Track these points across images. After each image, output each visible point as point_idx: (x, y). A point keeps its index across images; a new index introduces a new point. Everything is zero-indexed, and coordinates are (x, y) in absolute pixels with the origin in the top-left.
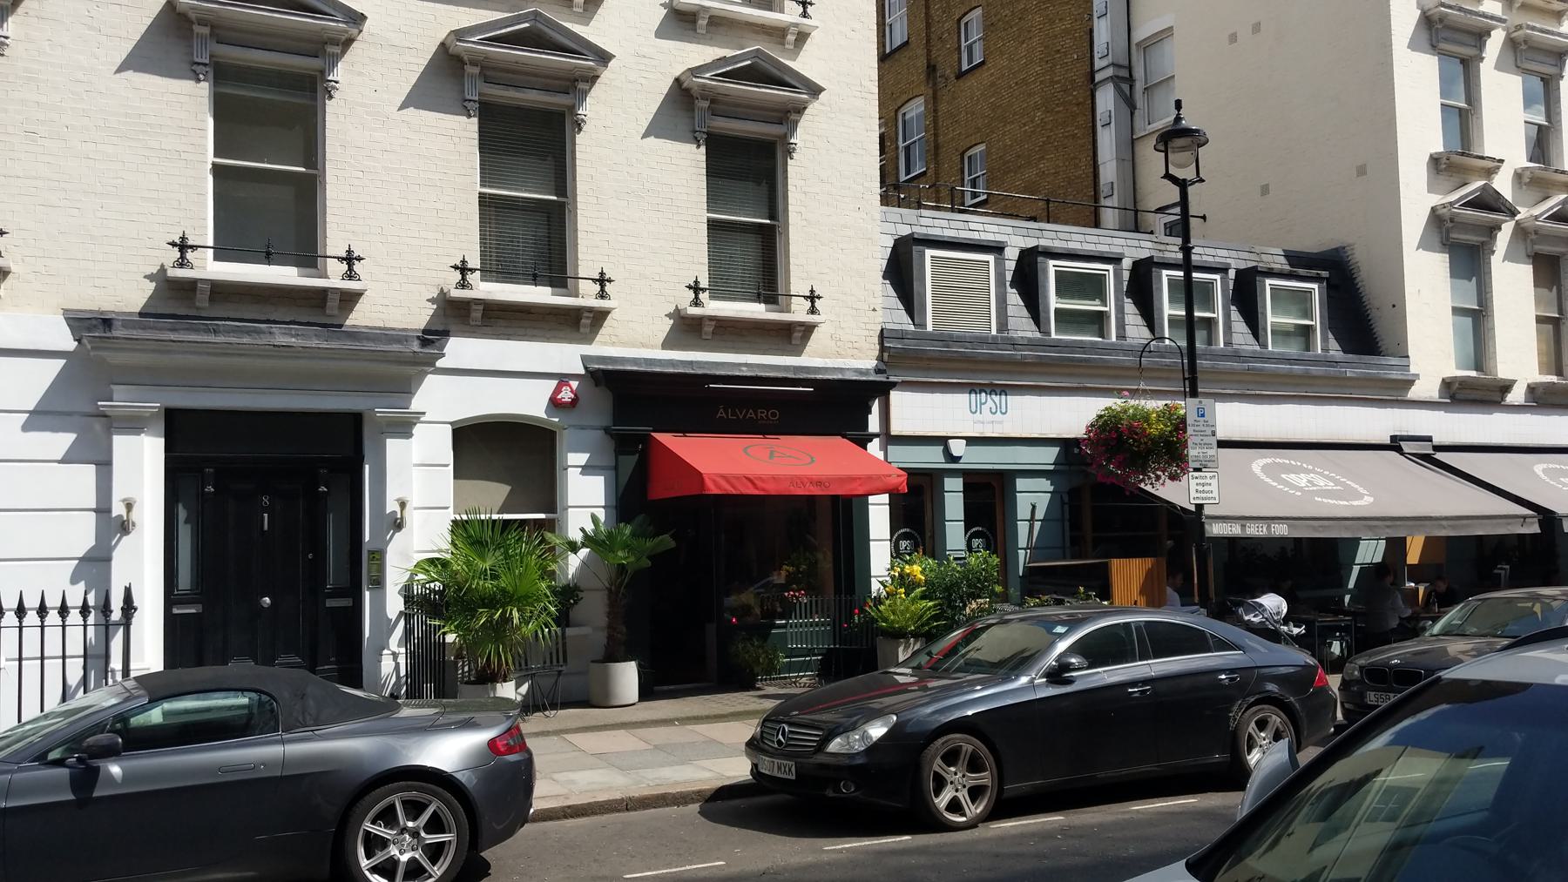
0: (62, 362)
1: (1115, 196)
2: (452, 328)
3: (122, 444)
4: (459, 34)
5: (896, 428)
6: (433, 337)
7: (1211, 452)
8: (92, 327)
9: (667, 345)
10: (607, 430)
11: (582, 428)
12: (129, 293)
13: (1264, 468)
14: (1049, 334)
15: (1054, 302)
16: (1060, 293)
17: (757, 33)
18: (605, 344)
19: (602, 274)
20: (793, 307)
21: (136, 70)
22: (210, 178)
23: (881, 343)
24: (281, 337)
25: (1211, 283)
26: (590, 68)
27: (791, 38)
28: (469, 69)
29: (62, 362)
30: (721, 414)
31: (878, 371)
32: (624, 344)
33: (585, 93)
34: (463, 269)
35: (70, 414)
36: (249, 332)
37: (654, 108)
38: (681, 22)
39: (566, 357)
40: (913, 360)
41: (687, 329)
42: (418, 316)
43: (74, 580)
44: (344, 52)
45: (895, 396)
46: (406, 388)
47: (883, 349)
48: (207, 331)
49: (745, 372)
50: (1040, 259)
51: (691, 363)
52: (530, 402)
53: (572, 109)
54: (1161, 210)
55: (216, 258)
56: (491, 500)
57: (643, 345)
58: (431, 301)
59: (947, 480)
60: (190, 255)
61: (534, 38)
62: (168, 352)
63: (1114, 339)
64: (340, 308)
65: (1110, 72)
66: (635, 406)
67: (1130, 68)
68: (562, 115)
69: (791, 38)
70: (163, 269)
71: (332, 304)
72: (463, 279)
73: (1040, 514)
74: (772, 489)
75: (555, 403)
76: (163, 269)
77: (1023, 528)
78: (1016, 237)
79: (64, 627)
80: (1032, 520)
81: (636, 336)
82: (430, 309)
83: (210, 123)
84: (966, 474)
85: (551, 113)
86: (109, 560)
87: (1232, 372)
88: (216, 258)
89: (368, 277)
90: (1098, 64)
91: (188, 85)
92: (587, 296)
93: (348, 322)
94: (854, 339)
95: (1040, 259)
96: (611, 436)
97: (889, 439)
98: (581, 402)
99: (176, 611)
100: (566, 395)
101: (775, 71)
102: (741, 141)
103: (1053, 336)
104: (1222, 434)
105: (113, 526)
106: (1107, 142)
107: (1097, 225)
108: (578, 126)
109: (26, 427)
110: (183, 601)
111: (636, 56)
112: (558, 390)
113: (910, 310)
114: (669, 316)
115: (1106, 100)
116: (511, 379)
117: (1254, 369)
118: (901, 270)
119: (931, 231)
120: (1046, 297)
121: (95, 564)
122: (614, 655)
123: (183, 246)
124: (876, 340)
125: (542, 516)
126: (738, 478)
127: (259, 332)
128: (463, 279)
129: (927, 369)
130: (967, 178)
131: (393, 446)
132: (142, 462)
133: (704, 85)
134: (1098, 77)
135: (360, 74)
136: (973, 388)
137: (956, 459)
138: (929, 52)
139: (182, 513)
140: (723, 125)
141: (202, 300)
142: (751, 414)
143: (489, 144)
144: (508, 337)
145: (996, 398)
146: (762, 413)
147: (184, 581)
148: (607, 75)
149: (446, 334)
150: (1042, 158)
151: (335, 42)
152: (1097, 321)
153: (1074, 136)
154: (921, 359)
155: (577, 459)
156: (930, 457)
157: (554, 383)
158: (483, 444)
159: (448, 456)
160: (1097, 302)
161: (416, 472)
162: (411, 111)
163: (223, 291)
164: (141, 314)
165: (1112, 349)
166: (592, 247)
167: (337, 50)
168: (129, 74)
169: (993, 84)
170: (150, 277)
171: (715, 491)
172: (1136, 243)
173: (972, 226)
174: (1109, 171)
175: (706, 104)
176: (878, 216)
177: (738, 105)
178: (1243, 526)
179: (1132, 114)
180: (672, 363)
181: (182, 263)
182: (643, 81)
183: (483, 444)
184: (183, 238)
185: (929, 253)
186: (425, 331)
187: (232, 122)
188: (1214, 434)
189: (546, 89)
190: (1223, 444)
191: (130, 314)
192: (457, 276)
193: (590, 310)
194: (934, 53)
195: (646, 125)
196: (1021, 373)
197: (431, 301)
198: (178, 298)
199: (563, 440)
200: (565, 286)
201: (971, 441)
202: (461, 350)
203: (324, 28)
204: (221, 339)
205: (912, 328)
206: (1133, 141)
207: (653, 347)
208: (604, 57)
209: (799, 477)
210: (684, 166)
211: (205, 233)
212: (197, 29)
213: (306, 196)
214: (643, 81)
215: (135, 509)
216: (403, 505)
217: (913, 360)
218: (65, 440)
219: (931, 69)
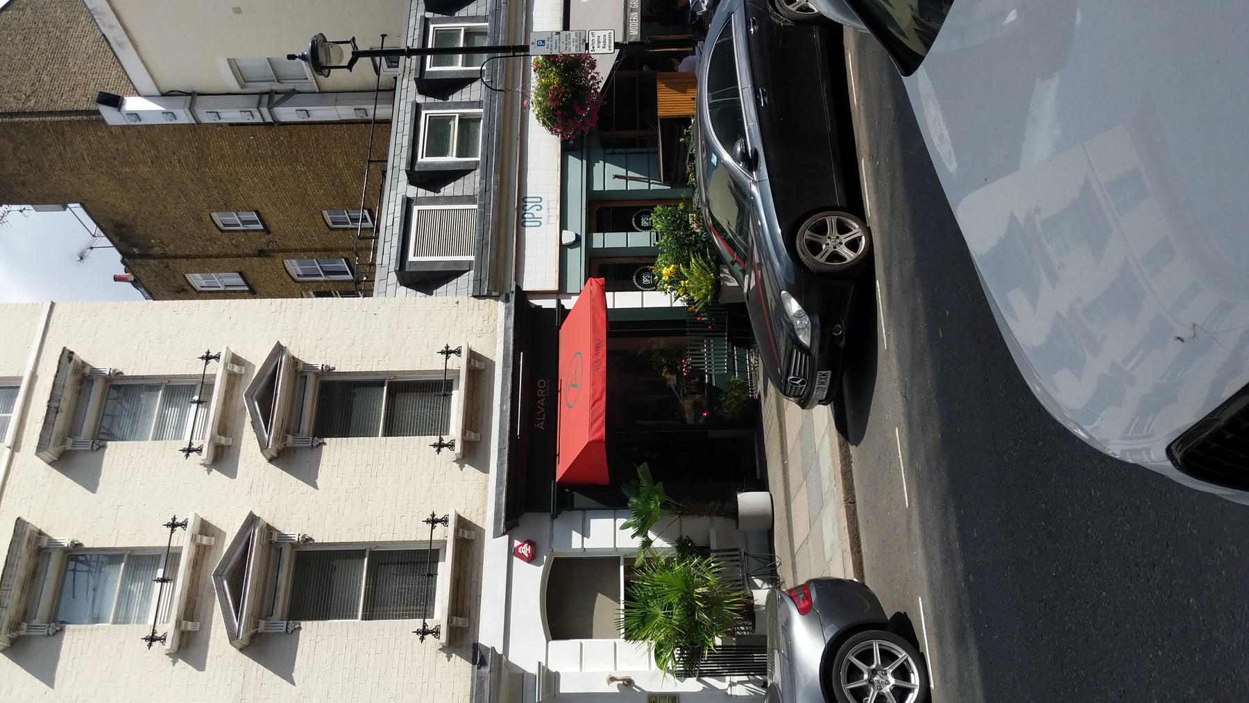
2: (471, 641)
4: (233, 637)
5: (554, 286)
6: (478, 656)
7: (573, 35)
9: (484, 468)
10: (554, 517)
11: (552, 536)
14: (477, 162)
15: (451, 158)
16: (444, 153)
17: (232, 397)
18: (484, 519)
19: (428, 521)
23: (484, 297)
25: (436, 31)
26: (261, 530)
27: (236, 369)
28: (261, 628)
30: (541, 426)
31: (507, 300)
32: (484, 504)
33: (281, 535)
34: (423, 632)
39: (494, 550)
40: (498, 273)
41: (472, 453)
42: (461, 668)
45: (526, 287)
46: (519, 677)
47: (489, 296)
49: (508, 406)
50: (417, 169)
51: (500, 450)
52: (530, 578)
53: (294, 545)
54: (377, 71)
58: (449, 658)
63: (481, 110)
65: (265, 110)
66: (535, 495)
67: (261, 94)
69: (236, 369)
72: (431, 632)
73: (622, 172)
74: (601, 385)
75: (532, 559)
77: (633, 186)
78: (399, 188)
80: (626, 178)
81: (478, 494)
82: (456, 658)
84: (590, 230)
90: (258, 119)
92: (446, 534)
95: (417, 169)
97: (562, 291)
100: (526, 550)
102: (319, 410)
103: (479, 159)
104: (558, 26)
106: (321, 113)
107: (389, 122)
108: (307, 540)
112: (521, 556)
113: (458, 274)
114: (462, 467)
115: (287, 113)
116: (512, 593)
118: (427, 281)
119: (394, 256)
120: (447, 164)
124: (482, 301)
125: (622, 568)
126: (592, 414)
128: (431, 632)
129: (506, 260)
130: (351, 226)
131: (565, 687)
133: (275, 439)
134: (269, 119)
136: (521, 224)
137: (578, 238)
138: (247, 255)
142: (541, 402)
144: (478, 596)
145: (529, 205)
148: (266, 517)
149: (476, 646)
150: (335, 165)
152: (467, 123)
154: (497, 266)
156: (576, 259)
157: (516, 559)
158: (565, 615)
159: (574, 643)
160: (451, 123)
161: (586, 669)
162: (295, 675)
165: (490, 112)
169: (274, 204)
172: (404, 92)
173: (389, 223)
174: (345, 112)
175: (290, 438)
176: (381, 299)
178: (632, 10)
180: (499, 466)
182: (271, 488)
183: (565, 615)
185: (411, 258)
186: (474, 663)
188: (558, 33)
190: (566, 26)
192: (429, 637)
193: (456, 531)
195: (306, 486)
196: (509, 184)
197: (449, 658)
200: (437, 551)
201: (563, 225)
202: (489, 634)
205: (472, 272)
207: (487, 481)
208: (252, 520)
214: (271, 488)
216: (612, 679)
217: (498, 273)
219: (261, 253)
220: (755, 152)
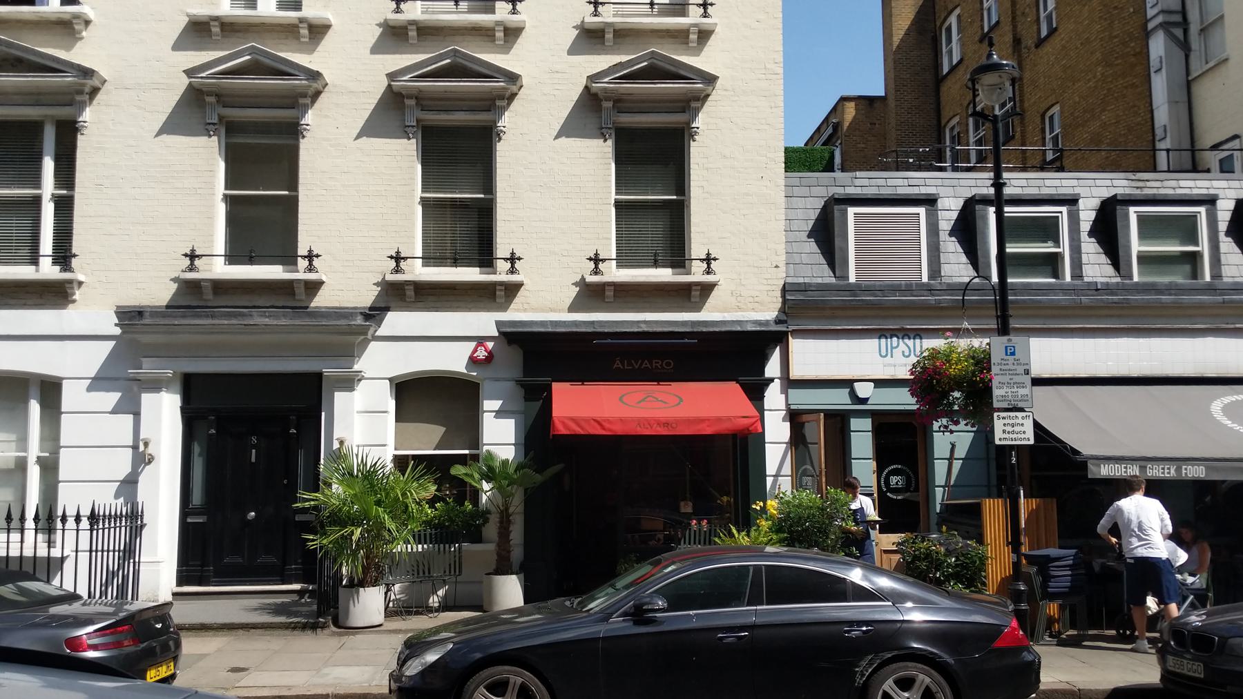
0: (114, 343)
1: (1168, 139)
2: (392, 305)
3: (147, 399)
4: (593, 78)
5: (796, 373)
6: (375, 313)
7: (1022, 391)
8: (130, 317)
9: (573, 308)
10: (519, 383)
11: (497, 380)
12: (160, 293)
13: (1226, 410)
14: (1131, 277)
15: (1136, 246)
16: (1143, 236)
17: (662, 37)
18: (518, 310)
19: (513, 254)
20: (693, 269)
21: (168, 134)
22: (613, 210)
23: (783, 296)
24: (258, 319)
25: (1193, 218)
26: (504, 88)
27: (693, 37)
28: (408, 102)
29: (114, 343)
30: (618, 364)
31: (778, 321)
32: (534, 310)
33: (697, 110)
34: (596, 260)
35: (116, 379)
36: (235, 316)
37: (366, 115)
38: (591, 38)
39: (484, 323)
40: (807, 310)
41: (592, 294)
42: (366, 296)
43: (117, 496)
44: (509, 105)
45: (795, 344)
46: (351, 352)
47: (785, 301)
48: (207, 316)
49: (645, 328)
50: (978, 207)
51: (593, 323)
52: (453, 360)
53: (688, 124)
54: (1215, 147)
55: (619, 266)
56: (427, 441)
57: (552, 310)
58: (377, 284)
59: (853, 421)
60: (601, 266)
61: (459, 70)
62: (172, 333)
63: (1068, 278)
64: (307, 294)
65: (1160, 19)
66: (542, 358)
67: (1184, 12)
68: (682, 130)
69: (693, 37)
70: (583, 279)
71: (300, 291)
72: (596, 267)
73: (961, 452)
74: (619, 429)
75: (473, 361)
76: (583, 279)
77: (940, 469)
78: (1092, 189)
79: (78, 530)
80: (951, 459)
81: (546, 301)
82: (376, 290)
83: (221, 166)
84: (875, 415)
85: (675, 129)
86: (136, 482)
87: (1200, 306)
88: (619, 266)
89: (721, 273)
90: (1150, 13)
91: (203, 140)
92: (697, 274)
93: (313, 305)
94: (757, 293)
95: (978, 207)
96: (522, 386)
97: (790, 384)
98: (495, 358)
99: (189, 520)
100: (482, 354)
101: (267, 61)
102: (647, 131)
103: (1136, 278)
104: (1038, 370)
105: (142, 458)
106: (1160, 86)
107: (1154, 169)
108: (692, 136)
109: (89, 389)
110: (196, 512)
111: (547, 71)
112: (475, 350)
113: (832, 264)
114: (576, 284)
115: (1158, 46)
116: (442, 342)
117: (1232, 301)
118: (825, 233)
119: (1162, 191)
120: (1129, 241)
121: (129, 485)
122: (503, 568)
123: (596, 260)
124: (779, 294)
125: (466, 452)
126: (587, 420)
127: (243, 315)
128: (596, 267)
129: (833, 317)
130: (1048, 136)
131: (340, 397)
132: (164, 414)
133: (605, 88)
134: (1151, 26)
135: (326, 116)
136: (882, 334)
137: (865, 401)
138: (1015, 27)
139: (196, 449)
140: (627, 119)
141: (208, 295)
142: (646, 364)
143: (622, 159)
144: (437, 309)
145: (910, 342)
146: (657, 363)
147: (197, 498)
148: (718, 95)
149: (387, 309)
150: (1104, 110)
151: (502, 98)
152: (1051, 263)
153: (1133, 86)
154: (824, 309)
155: (490, 405)
156: (838, 399)
157: (473, 344)
158: (415, 395)
159: (391, 405)
160: (1050, 244)
161: (357, 417)
162: (563, 140)
163: (222, 287)
164: (167, 307)
165: (1065, 290)
166: (703, 234)
167: (504, 103)
168: (164, 137)
169: (1064, 47)
170: (576, 284)
171: (563, 431)
172: (1108, 183)
173: (912, 182)
174: (1162, 115)
175: (610, 104)
176: (782, 182)
177: (643, 101)
178: (1143, 468)
179: (1187, 57)
180: (575, 323)
181: (596, 272)
182: (556, 92)
183: (415, 395)
184: (596, 254)
185: (852, 211)
186: (371, 309)
187: (239, 166)
188: (1027, 372)
189: (472, 110)
190: (1037, 382)
191: (160, 307)
192: (393, 264)
193: (501, 283)
194: (1019, 27)
195: (558, 127)
196: (939, 317)
197: (377, 284)
198: (195, 295)
199: (486, 387)
200: (684, 267)
201: (879, 383)
202: (397, 321)
203: (295, 86)
204: (216, 322)
205: (833, 280)
206: (1189, 84)
207: (560, 311)
208: (710, 79)
209: (646, 419)
210: (596, 159)
211: (219, 244)
212: (408, 102)
213: (675, 218)
214: (556, 92)
215: (150, 446)
216: (342, 443)
217: (807, 310)
218: (114, 397)
219: (1017, 42)
220: (652, 621)
